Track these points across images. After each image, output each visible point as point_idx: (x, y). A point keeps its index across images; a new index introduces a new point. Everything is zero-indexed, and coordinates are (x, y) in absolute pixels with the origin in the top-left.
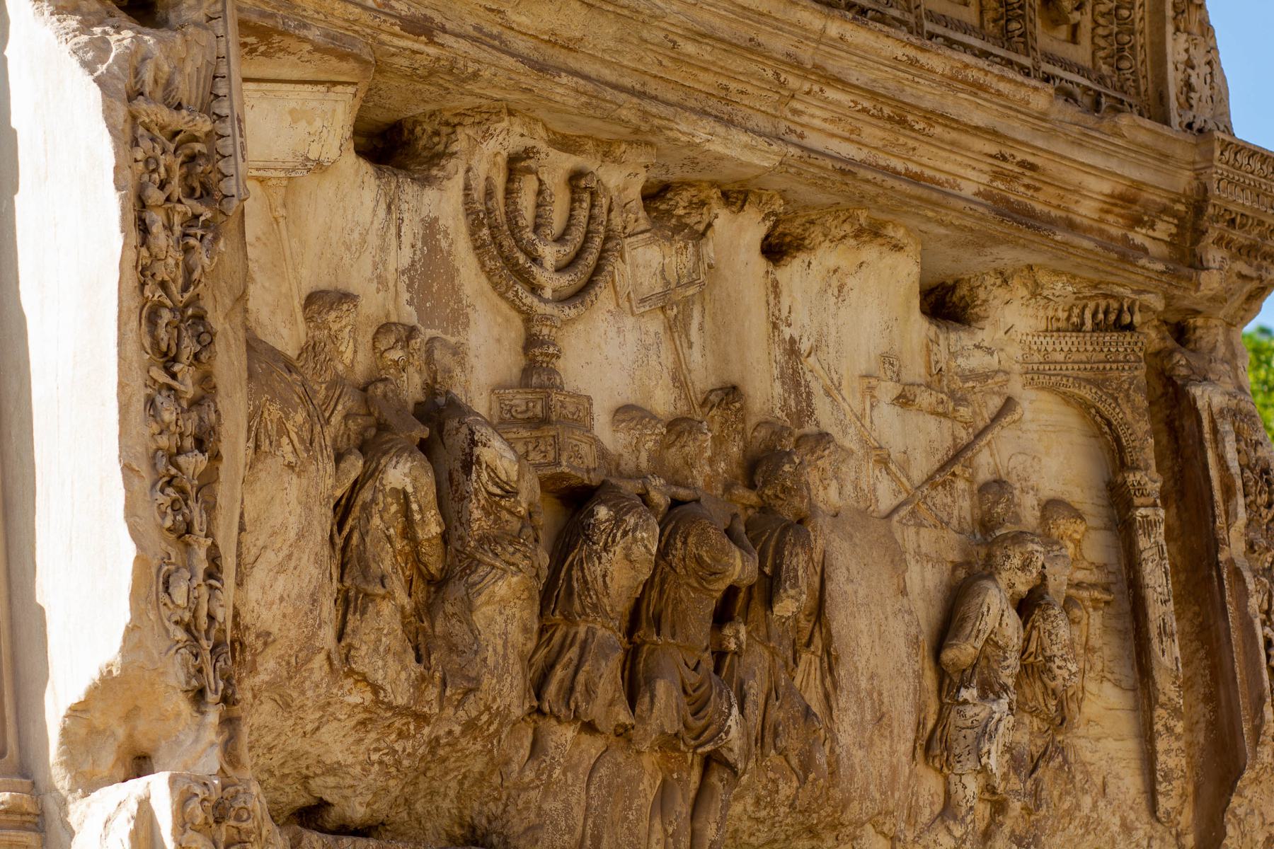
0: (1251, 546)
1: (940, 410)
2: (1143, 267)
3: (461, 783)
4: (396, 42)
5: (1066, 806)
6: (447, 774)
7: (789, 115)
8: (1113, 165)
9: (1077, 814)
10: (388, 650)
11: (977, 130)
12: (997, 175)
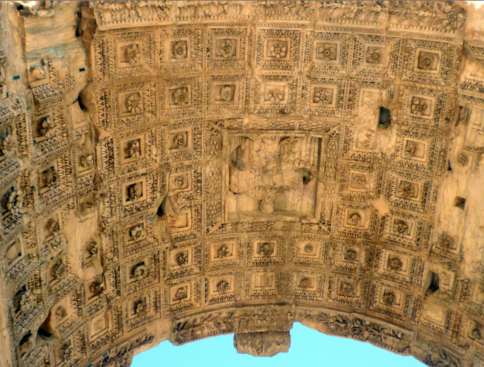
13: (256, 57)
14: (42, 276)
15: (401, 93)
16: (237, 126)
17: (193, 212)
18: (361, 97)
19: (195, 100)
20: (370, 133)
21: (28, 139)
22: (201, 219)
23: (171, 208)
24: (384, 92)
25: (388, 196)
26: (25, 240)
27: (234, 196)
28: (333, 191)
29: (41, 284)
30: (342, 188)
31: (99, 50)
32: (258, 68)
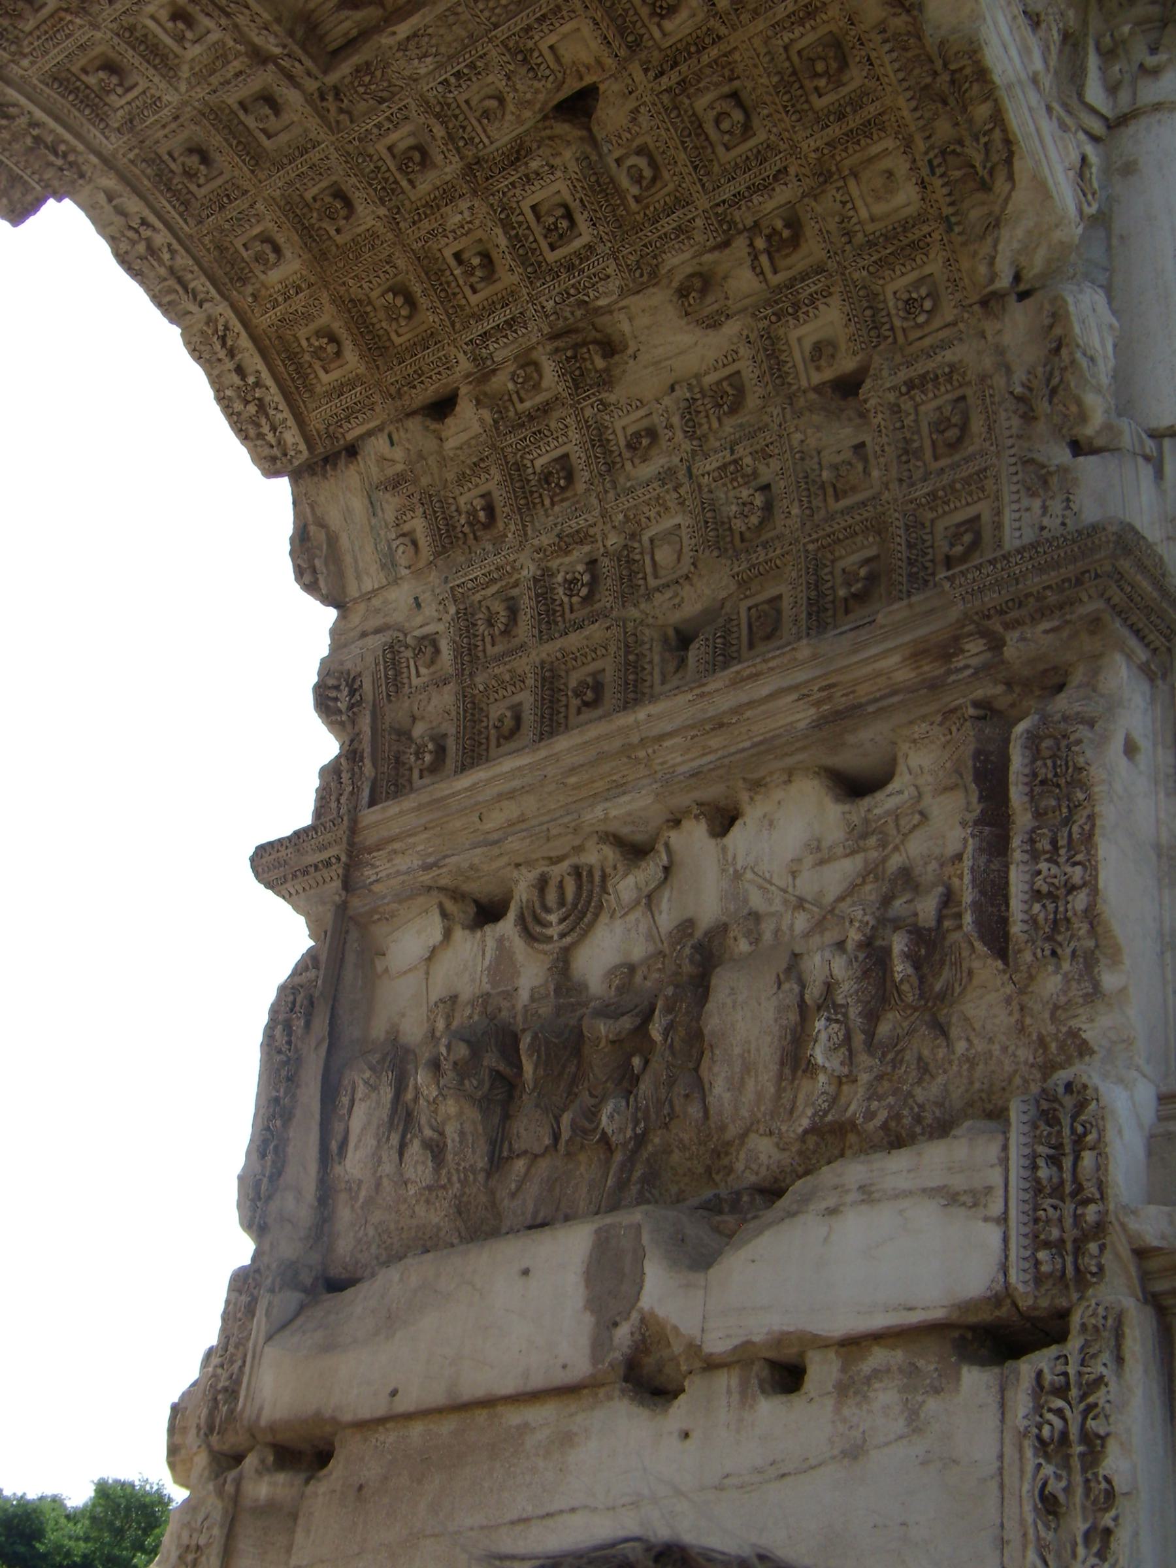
0: (1038, 815)
1: (848, 851)
2: (954, 682)
3: (486, 1208)
4: (427, 877)
5: (940, 1055)
6: (477, 1207)
7: (660, 767)
8: (889, 644)
9: (952, 1057)
10: (417, 1162)
11: (773, 696)
12: (818, 703)
13: (156, 117)
14: (715, 465)
16: (297, 64)
17: (537, 38)
21: (487, 570)
26: (654, 521)
29: (730, 463)
31: (346, 426)
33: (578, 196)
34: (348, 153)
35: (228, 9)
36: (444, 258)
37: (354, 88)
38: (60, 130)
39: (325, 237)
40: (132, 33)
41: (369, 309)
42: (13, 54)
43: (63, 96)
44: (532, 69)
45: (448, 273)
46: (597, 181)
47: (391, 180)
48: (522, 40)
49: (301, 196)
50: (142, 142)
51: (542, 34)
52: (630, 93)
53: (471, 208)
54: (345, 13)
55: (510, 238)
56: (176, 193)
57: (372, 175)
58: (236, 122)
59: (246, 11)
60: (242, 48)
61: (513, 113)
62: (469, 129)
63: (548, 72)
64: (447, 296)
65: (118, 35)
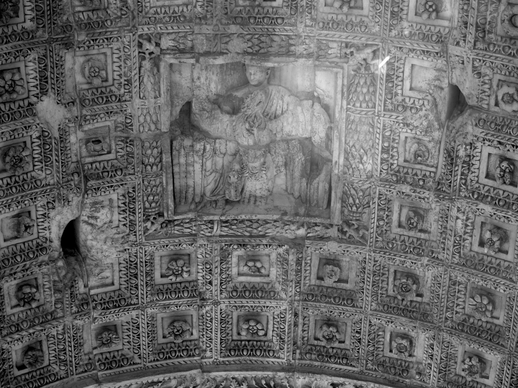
15: (59, 306)
16: (316, 228)
17: (400, 92)
18: (117, 274)
19: (383, 274)
20: (92, 221)
22: (387, 81)
23: (440, 107)
24: (82, 290)
25: (43, 136)
27: (319, 92)
28: (142, 119)
30: (127, 126)
32: (283, 308)
33: (495, 143)
34: (381, 248)
35: (261, 233)
36: (477, 253)
37: (351, 211)
38: (254, 374)
39: (418, 305)
40: (237, 291)
41: (471, 320)
42: (199, 355)
43: (241, 356)
44: (411, 108)
45: (485, 257)
46: (496, 124)
47: (415, 240)
48: (394, 100)
49: (388, 296)
50: (295, 343)
51: (400, 87)
52: (463, 63)
53: (459, 210)
54: (315, 181)
55: (490, 203)
56: (336, 356)
57: (403, 247)
58: (325, 290)
59: (268, 226)
60: (286, 247)
61: (430, 141)
62: (419, 172)
63: (421, 102)
64: (495, 269)
65: (230, 298)
